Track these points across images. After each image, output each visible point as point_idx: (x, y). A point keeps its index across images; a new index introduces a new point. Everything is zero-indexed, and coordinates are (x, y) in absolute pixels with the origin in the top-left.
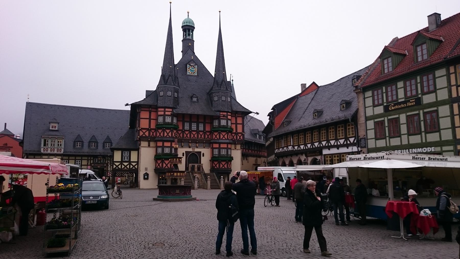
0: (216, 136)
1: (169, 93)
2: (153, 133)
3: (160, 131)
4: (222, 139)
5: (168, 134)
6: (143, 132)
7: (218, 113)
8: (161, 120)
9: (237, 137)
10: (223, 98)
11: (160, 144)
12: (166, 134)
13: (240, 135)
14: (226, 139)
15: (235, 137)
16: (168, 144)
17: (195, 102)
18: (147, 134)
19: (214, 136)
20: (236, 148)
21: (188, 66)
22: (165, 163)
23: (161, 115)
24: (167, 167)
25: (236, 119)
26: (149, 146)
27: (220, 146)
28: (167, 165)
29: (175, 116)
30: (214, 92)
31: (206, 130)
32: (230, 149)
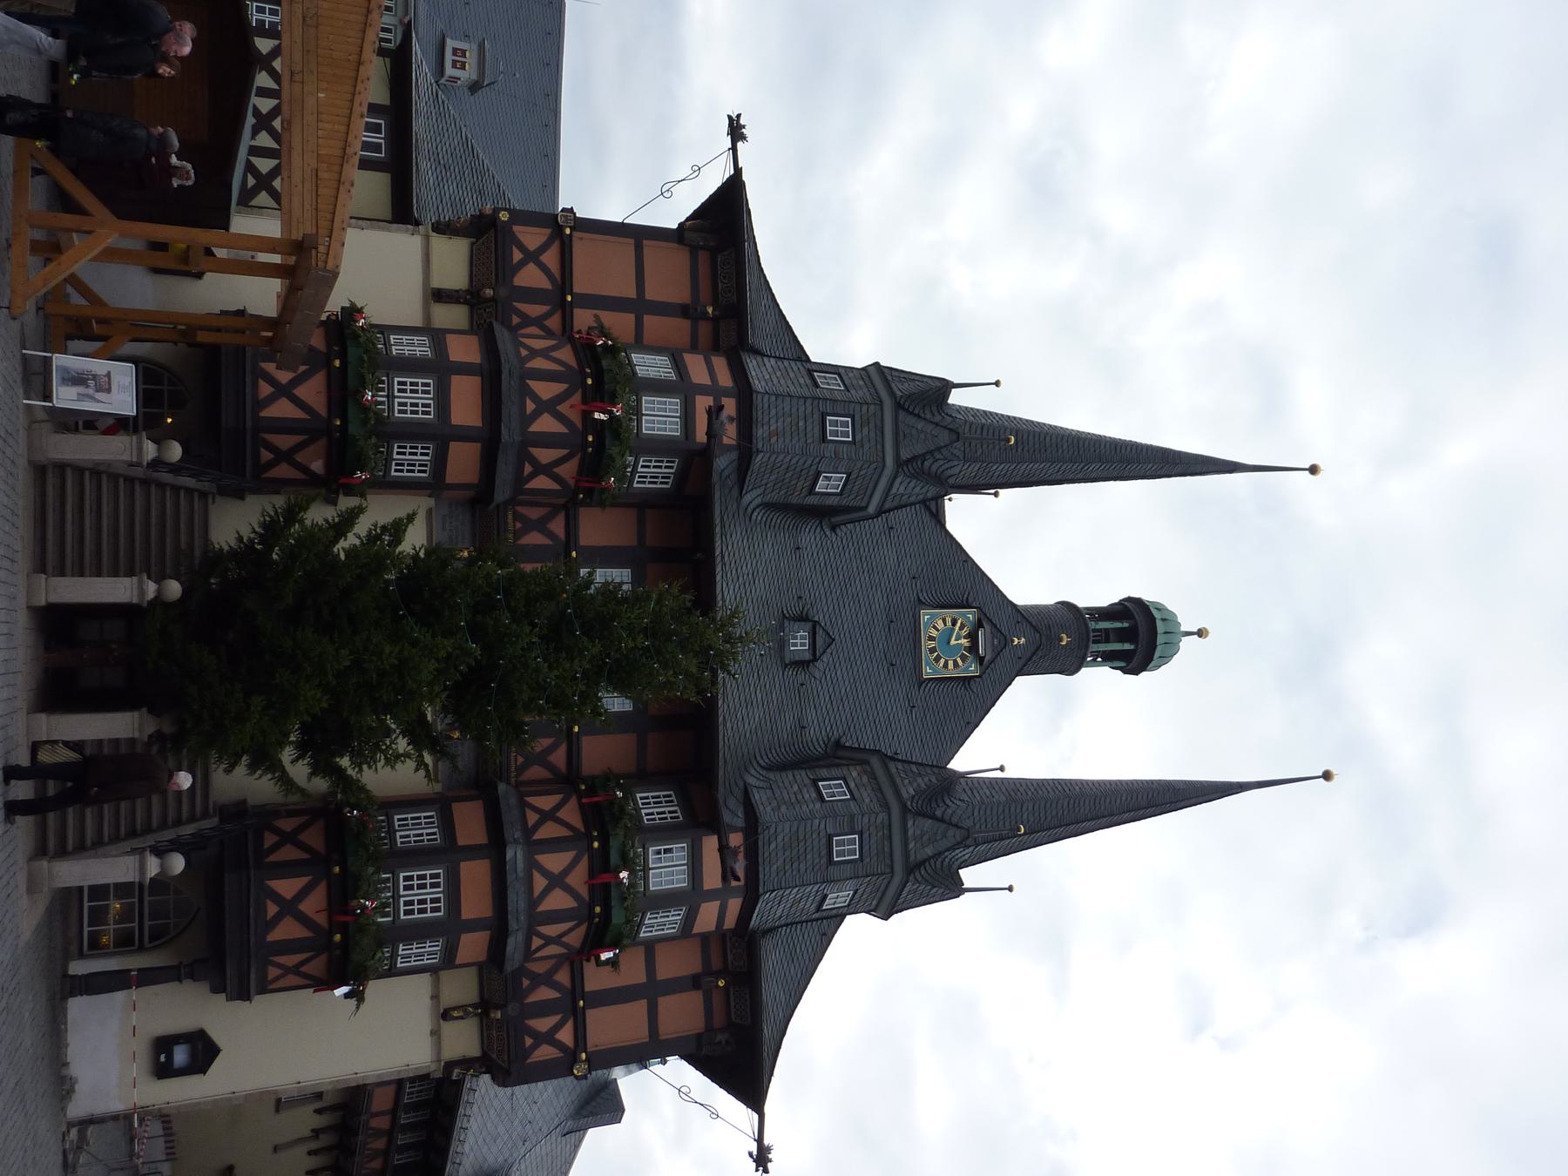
0: (547, 816)
1: (839, 429)
2: (538, 322)
3: (566, 354)
4: (532, 865)
5: (549, 407)
6: (543, 248)
7: (733, 815)
8: (650, 365)
9: (544, 1009)
10: (847, 847)
11: (464, 350)
12: (546, 390)
13: (566, 1036)
14: (533, 903)
15: (545, 994)
16: (466, 407)
17: (782, 645)
18: (530, 277)
19: (546, 802)
20: (446, 1015)
21: (971, 615)
22: (296, 382)
23: (678, 365)
24: (265, 389)
25: (695, 982)
26: (439, 296)
27: (472, 852)
28: (284, 391)
29: (682, 477)
30: (873, 776)
31: (586, 742)
32: (449, 960)
